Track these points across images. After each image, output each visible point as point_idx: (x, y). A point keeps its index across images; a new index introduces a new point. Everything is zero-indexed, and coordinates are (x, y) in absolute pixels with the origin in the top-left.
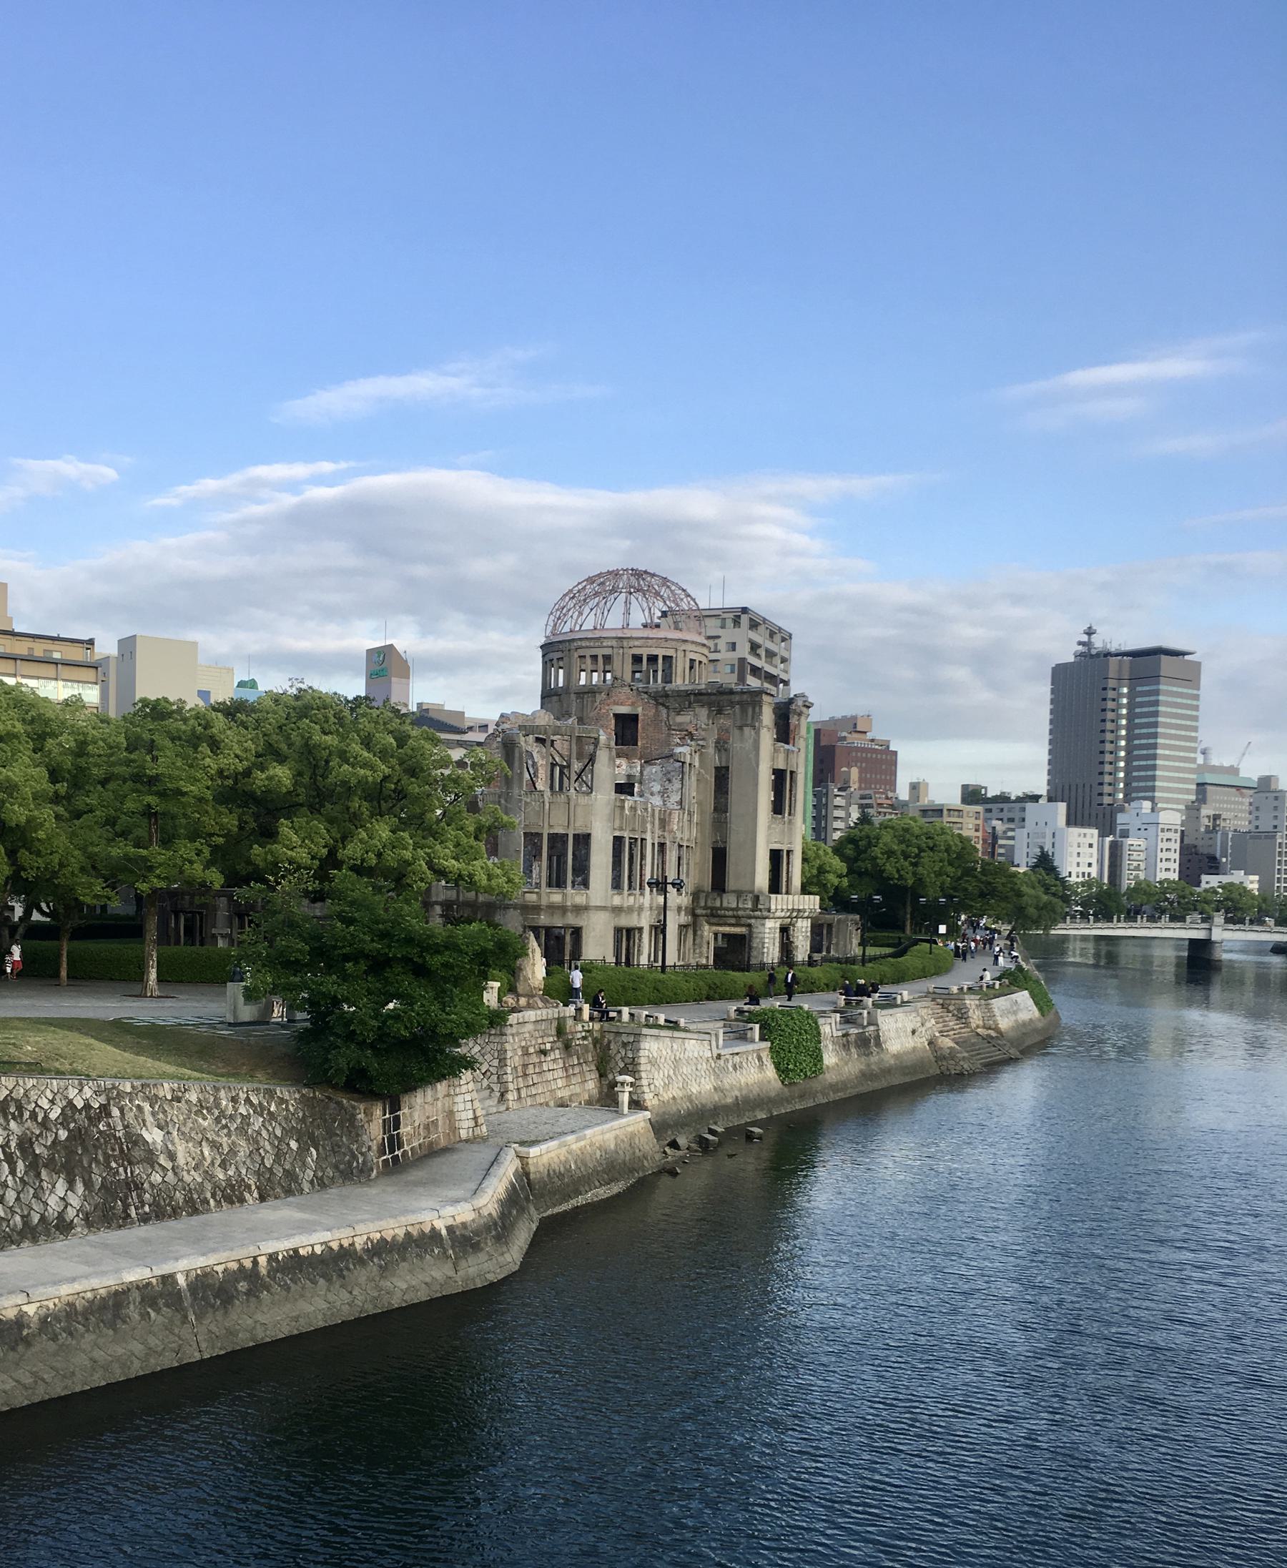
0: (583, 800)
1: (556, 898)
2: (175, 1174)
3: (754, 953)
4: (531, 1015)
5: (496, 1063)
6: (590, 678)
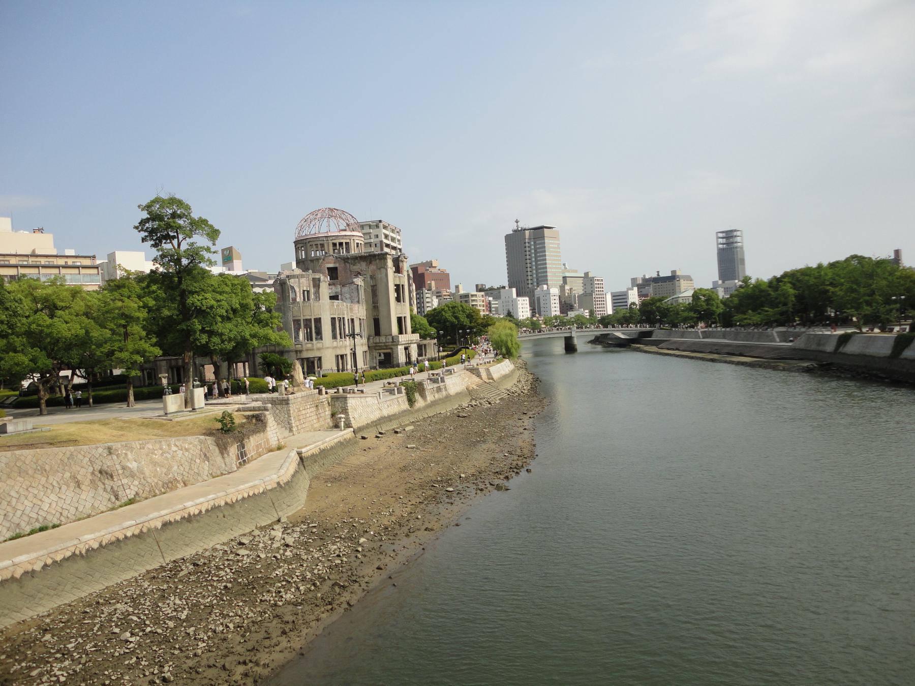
0: (316, 304)
1: (309, 346)
2: (144, 480)
3: (395, 359)
4: (298, 395)
5: (286, 416)
6: (315, 254)
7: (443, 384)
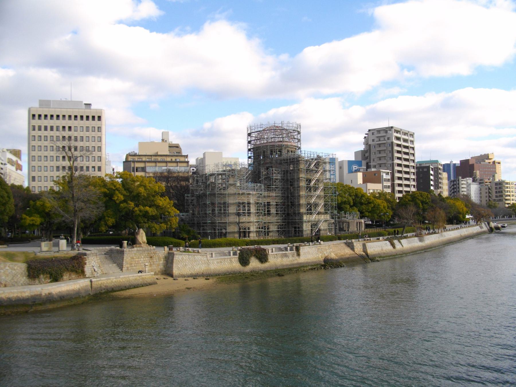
7: (291, 252)
